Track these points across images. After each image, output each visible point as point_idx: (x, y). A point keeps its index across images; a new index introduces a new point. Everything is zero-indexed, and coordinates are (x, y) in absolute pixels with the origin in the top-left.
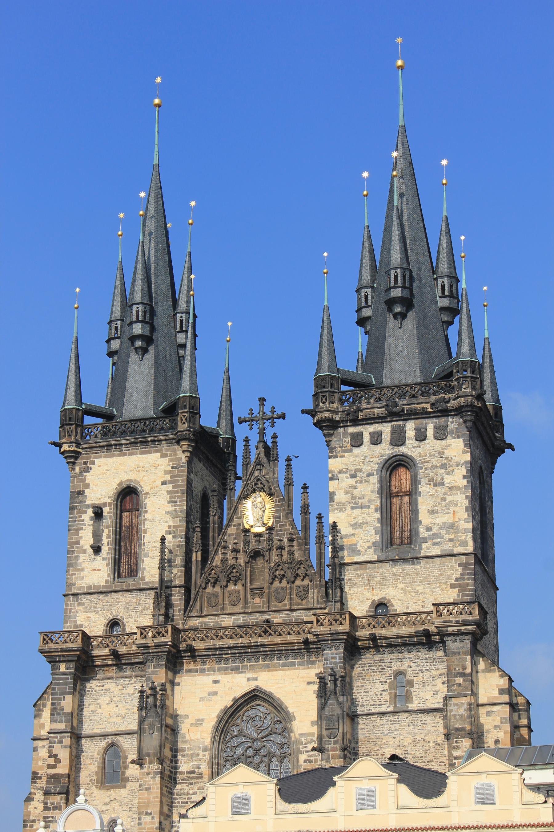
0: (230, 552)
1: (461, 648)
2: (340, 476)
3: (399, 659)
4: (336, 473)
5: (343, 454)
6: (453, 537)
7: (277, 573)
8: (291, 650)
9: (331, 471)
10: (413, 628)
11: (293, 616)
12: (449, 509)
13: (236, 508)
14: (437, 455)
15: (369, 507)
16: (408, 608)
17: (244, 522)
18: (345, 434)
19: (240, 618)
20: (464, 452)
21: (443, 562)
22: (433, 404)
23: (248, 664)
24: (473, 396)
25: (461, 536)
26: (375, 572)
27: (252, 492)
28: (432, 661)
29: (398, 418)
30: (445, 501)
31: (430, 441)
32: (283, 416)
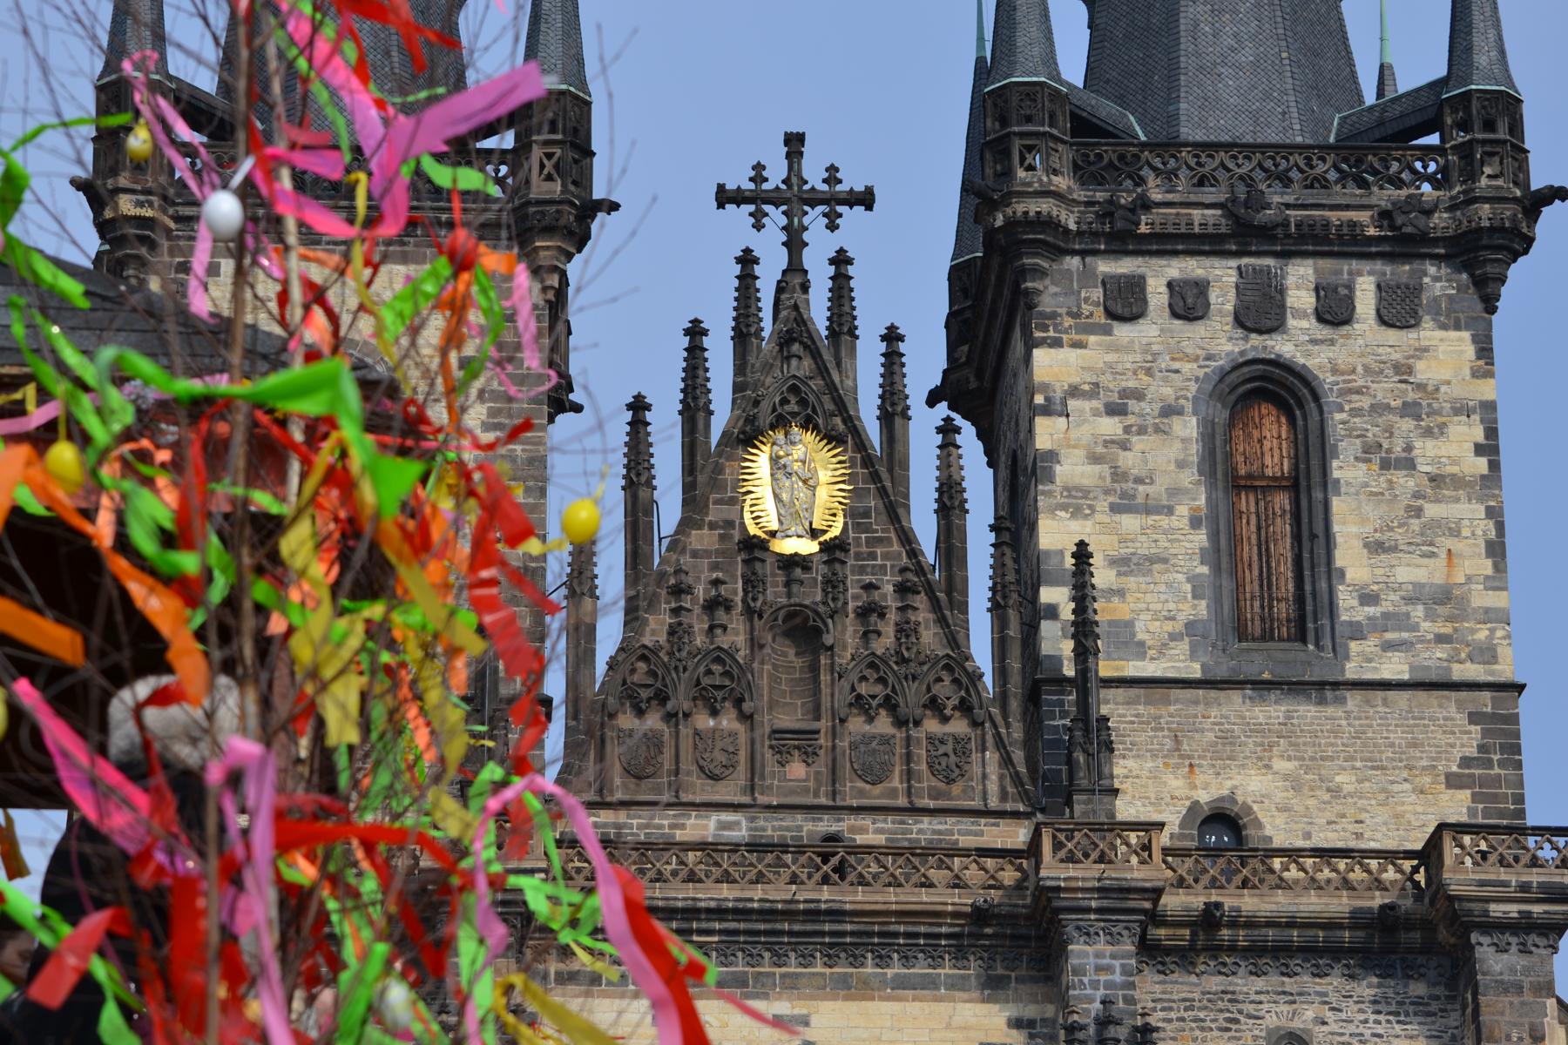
0: (697, 610)
1: (1527, 971)
2: (1073, 404)
3: (1284, 993)
4: (1059, 394)
5: (1083, 337)
6: (1447, 629)
7: (863, 689)
8: (927, 936)
9: (1045, 388)
10: (1345, 900)
11: (920, 831)
12: (1431, 544)
13: (719, 470)
14: (1390, 372)
15: (1170, 511)
16: (1308, 836)
17: (747, 516)
18: (1087, 276)
19: (738, 823)
20: (1476, 374)
21: (1420, 705)
22: (1385, 216)
23: (777, 970)
24: (1515, 200)
25: (1473, 631)
26: (1196, 716)
27: (773, 427)
28: (1393, 1008)
29: (1266, 248)
30: (1418, 517)
31: (1365, 327)
32: (865, 199)
